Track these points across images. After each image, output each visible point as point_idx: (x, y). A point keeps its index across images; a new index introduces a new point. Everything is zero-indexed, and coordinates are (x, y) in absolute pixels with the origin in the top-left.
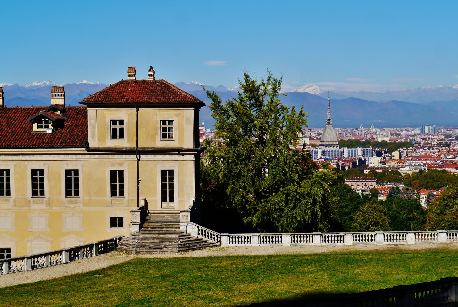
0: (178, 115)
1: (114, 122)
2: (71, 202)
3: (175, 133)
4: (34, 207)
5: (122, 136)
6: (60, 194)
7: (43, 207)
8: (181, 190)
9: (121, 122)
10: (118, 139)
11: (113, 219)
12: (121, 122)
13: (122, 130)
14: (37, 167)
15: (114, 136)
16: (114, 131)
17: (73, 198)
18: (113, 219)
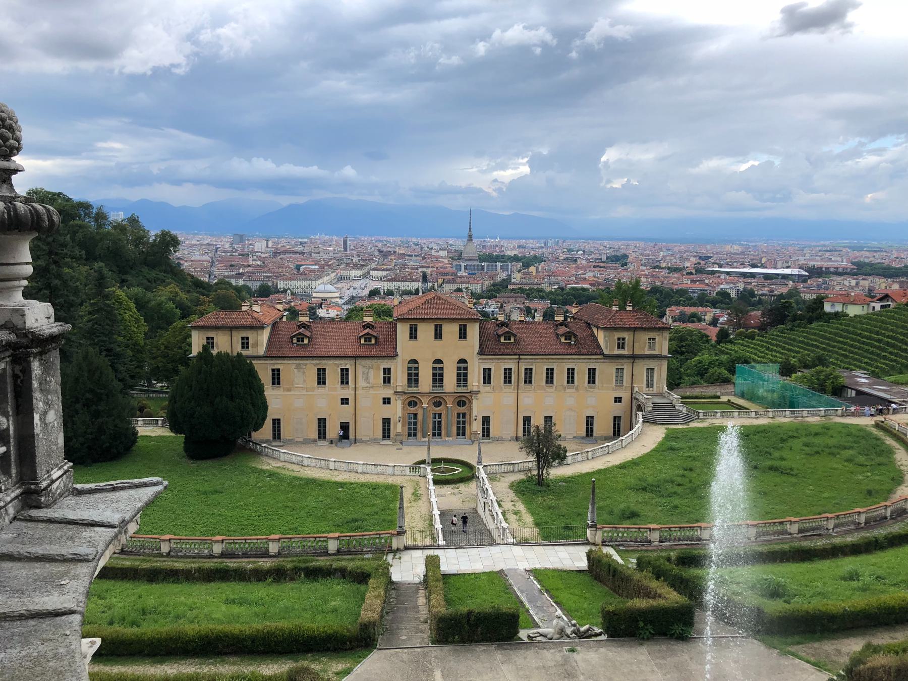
0: (658, 335)
1: (619, 339)
2: (591, 388)
3: (657, 346)
4: (568, 391)
5: (623, 348)
6: (584, 383)
7: (574, 390)
8: (659, 380)
9: (624, 339)
10: (620, 349)
11: (616, 398)
12: (624, 339)
13: (623, 344)
14: (570, 366)
15: (619, 347)
16: (619, 344)
17: (592, 385)
18: (616, 398)
